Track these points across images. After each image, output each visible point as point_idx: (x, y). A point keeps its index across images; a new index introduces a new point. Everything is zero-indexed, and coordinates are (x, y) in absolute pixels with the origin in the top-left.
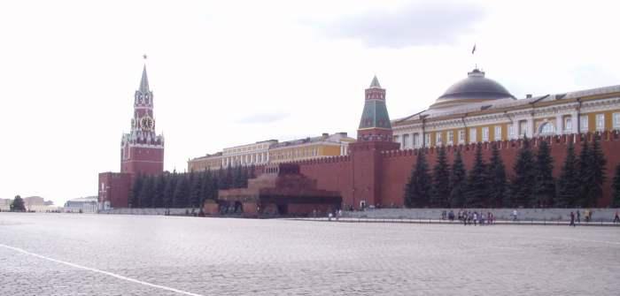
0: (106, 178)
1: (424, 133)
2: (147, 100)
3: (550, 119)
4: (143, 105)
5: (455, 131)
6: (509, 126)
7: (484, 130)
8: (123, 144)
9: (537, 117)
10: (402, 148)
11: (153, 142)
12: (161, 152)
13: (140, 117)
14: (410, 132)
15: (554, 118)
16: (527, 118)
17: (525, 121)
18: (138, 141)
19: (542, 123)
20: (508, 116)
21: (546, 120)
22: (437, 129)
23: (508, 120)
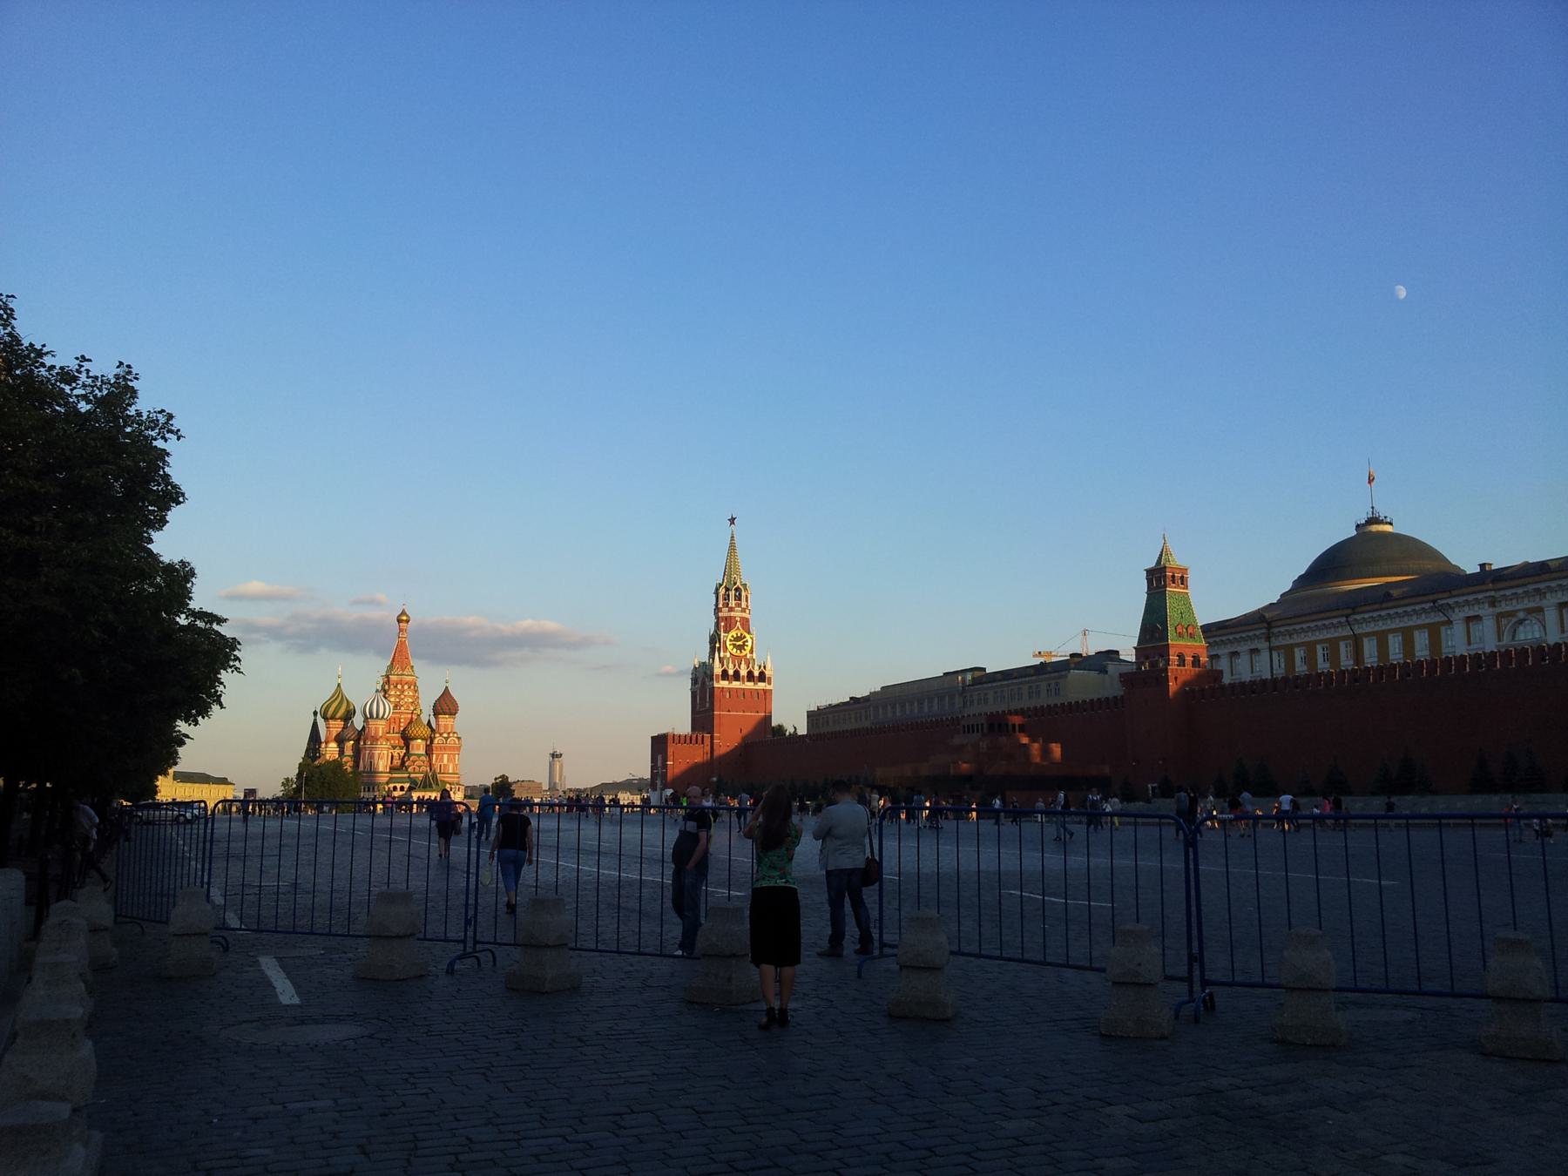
1: (1271, 649)
3: (1530, 611)
5: (1333, 644)
6: (1443, 629)
7: (1390, 643)
8: (694, 681)
9: (1504, 607)
10: (1227, 680)
11: (750, 676)
14: (1243, 648)
15: (1540, 610)
16: (1481, 612)
17: (1478, 618)
18: (725, 675)
20: (1441, 609)
21: (1521, 615)
22: (1297, 639)
23: (1441, 618)
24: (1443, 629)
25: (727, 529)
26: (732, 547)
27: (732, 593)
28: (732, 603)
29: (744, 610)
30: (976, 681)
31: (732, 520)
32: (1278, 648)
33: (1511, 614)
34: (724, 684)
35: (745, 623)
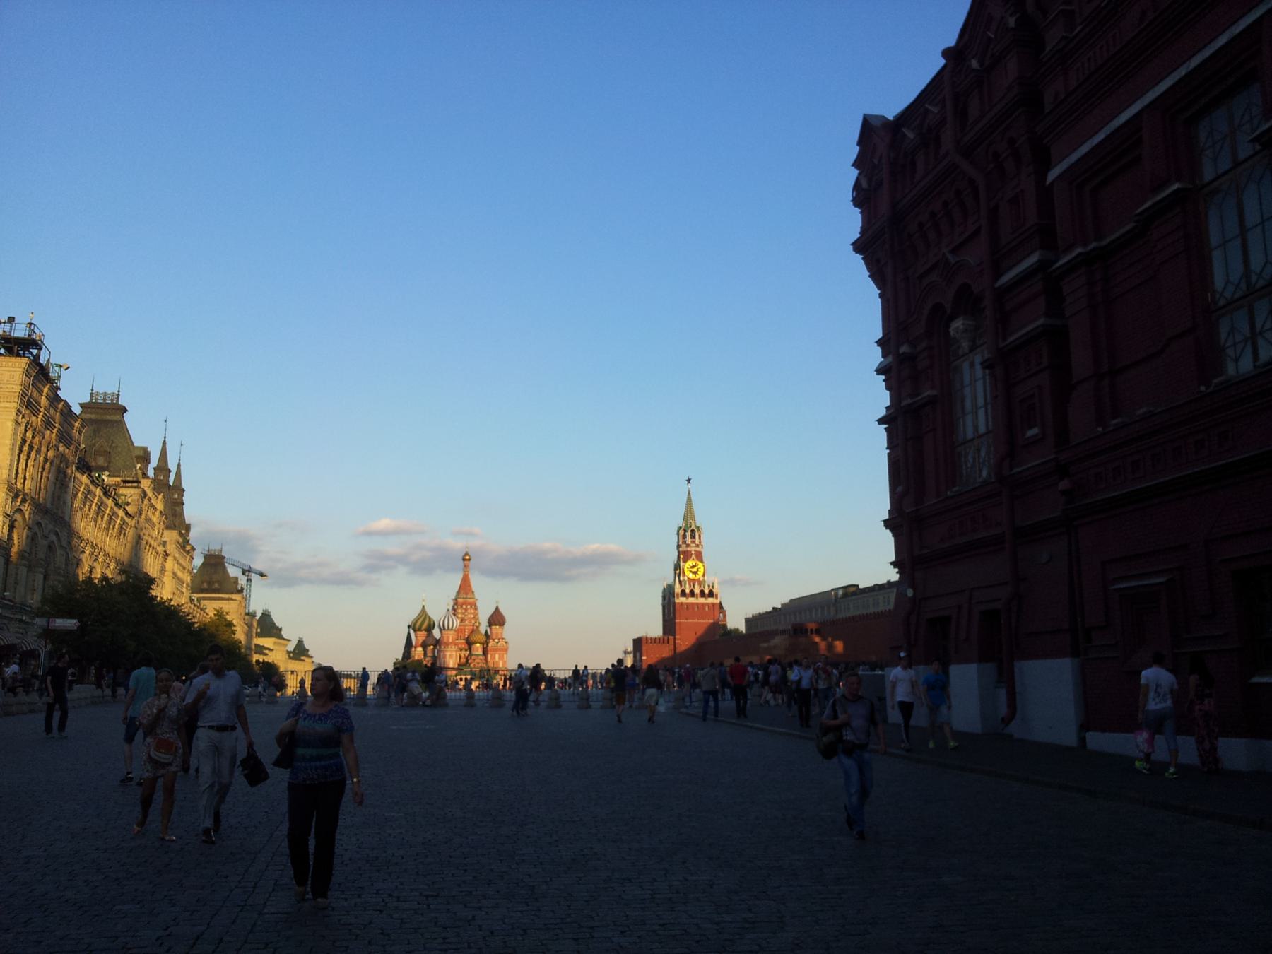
8: (664, 598)
11: (702, 594)
18: (683, 593)
25: (686, 487)
26: (689, 500)
27: (688, 534)
28: (689, 540)
30: (845, 595)
31: (689, 481)
34: (683, 600)
35: (699, 556)
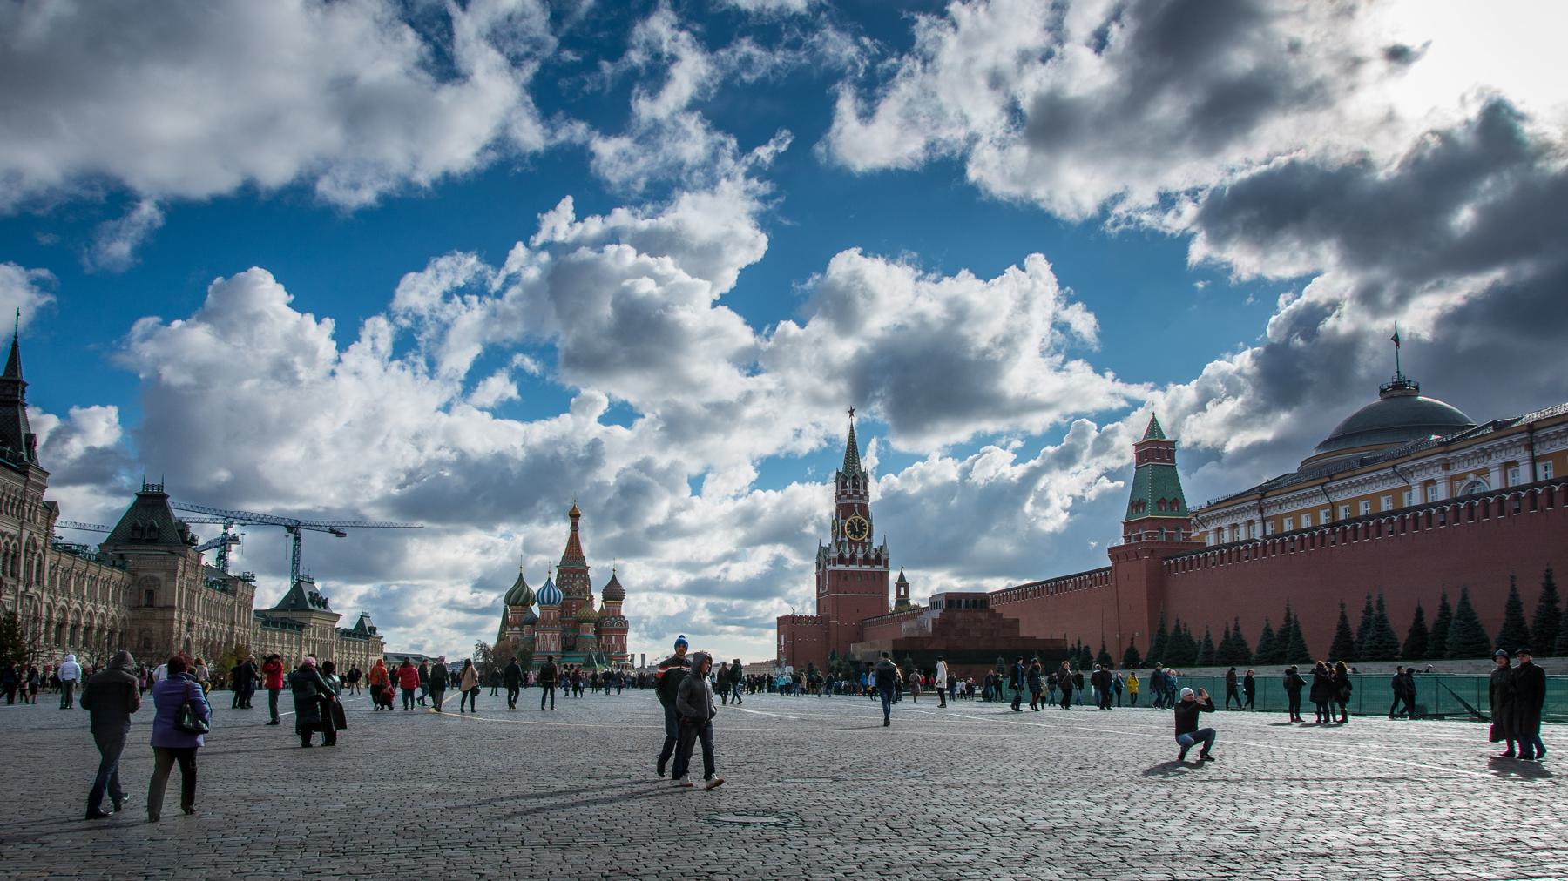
0: (788, 625)
1: (1264, 521)
2: (856, 486)
4: (850, 497)
6: (1405, 494)
9: (1456, 470)
11: (867, 560)
12: (883, 576)
13: (844, 518)
19: (1466, 483)
20: (1404, 474)
21: (1472, 477)
22: (1286, 509)
24: (1405, 494)
29: (861, 497)
32: (1270, 519)
33: (1463, 477)
